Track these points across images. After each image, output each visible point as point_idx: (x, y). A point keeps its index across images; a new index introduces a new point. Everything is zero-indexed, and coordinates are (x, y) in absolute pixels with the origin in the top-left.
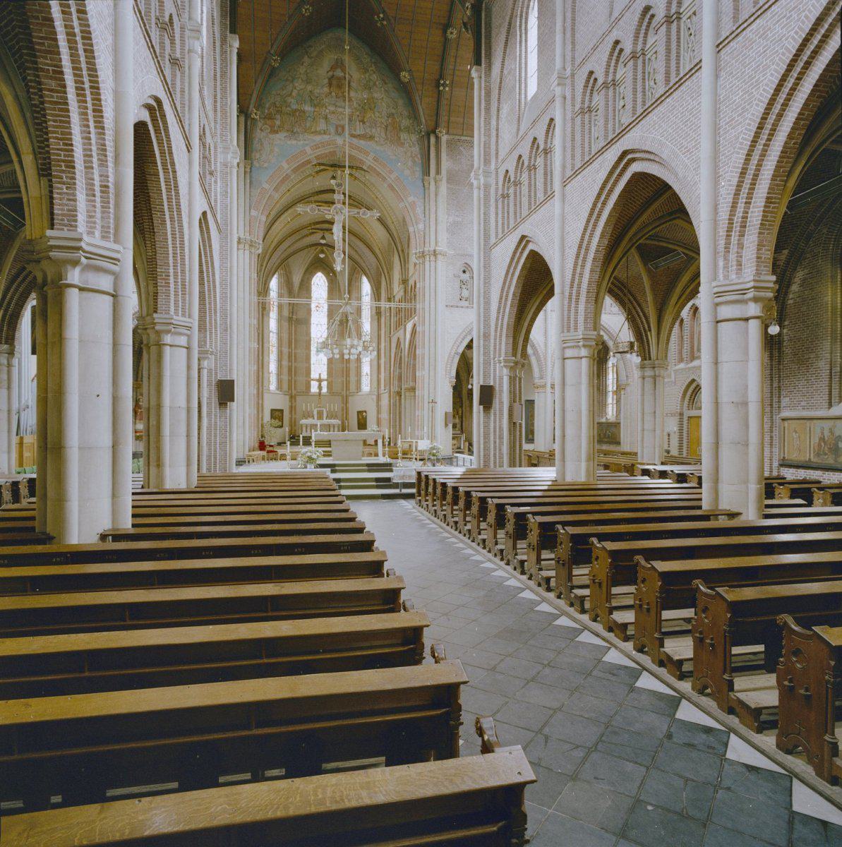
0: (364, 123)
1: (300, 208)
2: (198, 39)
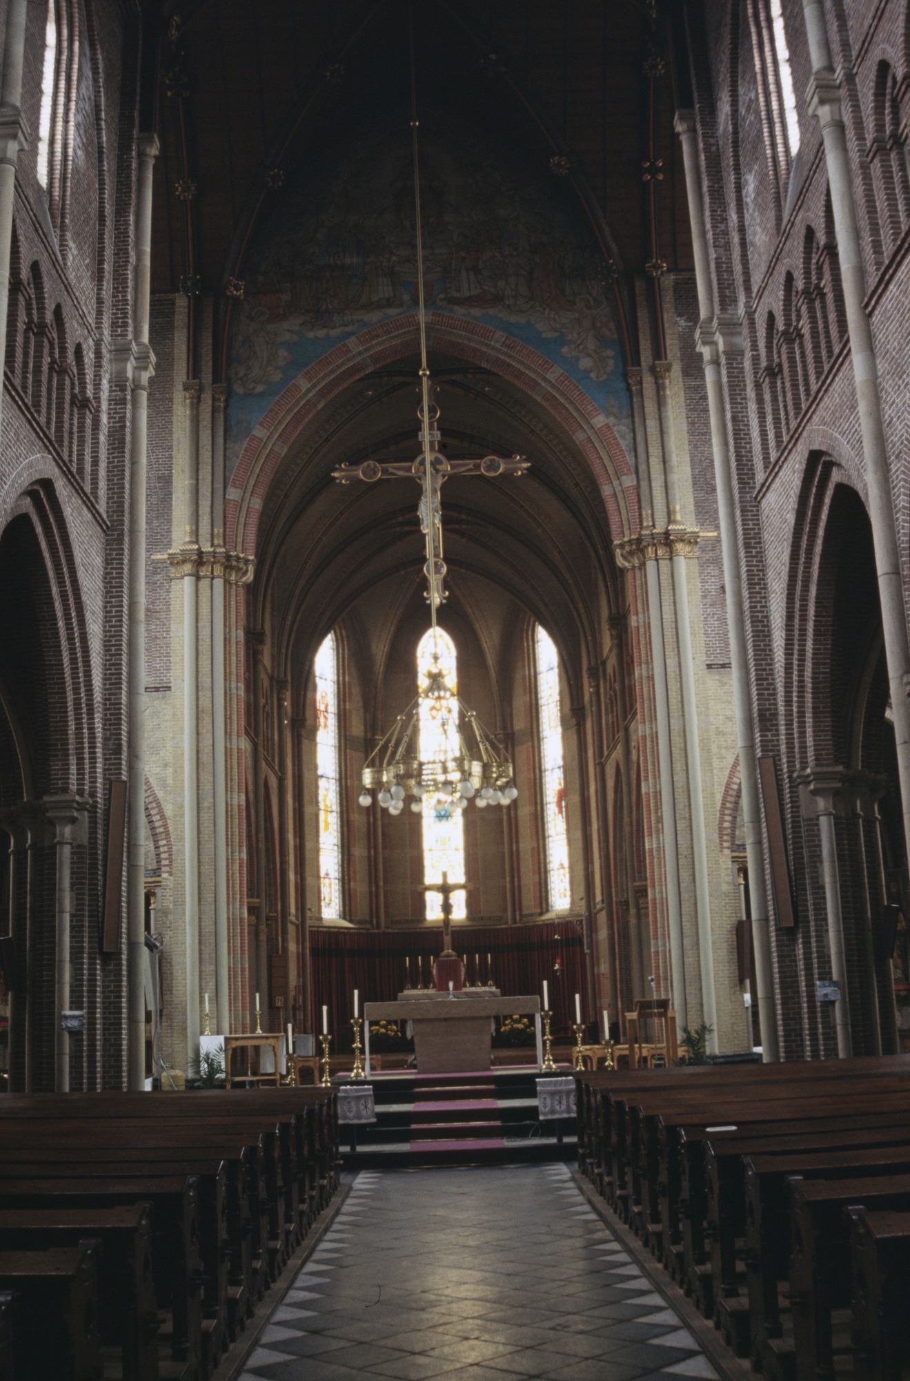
2: (15, 137)
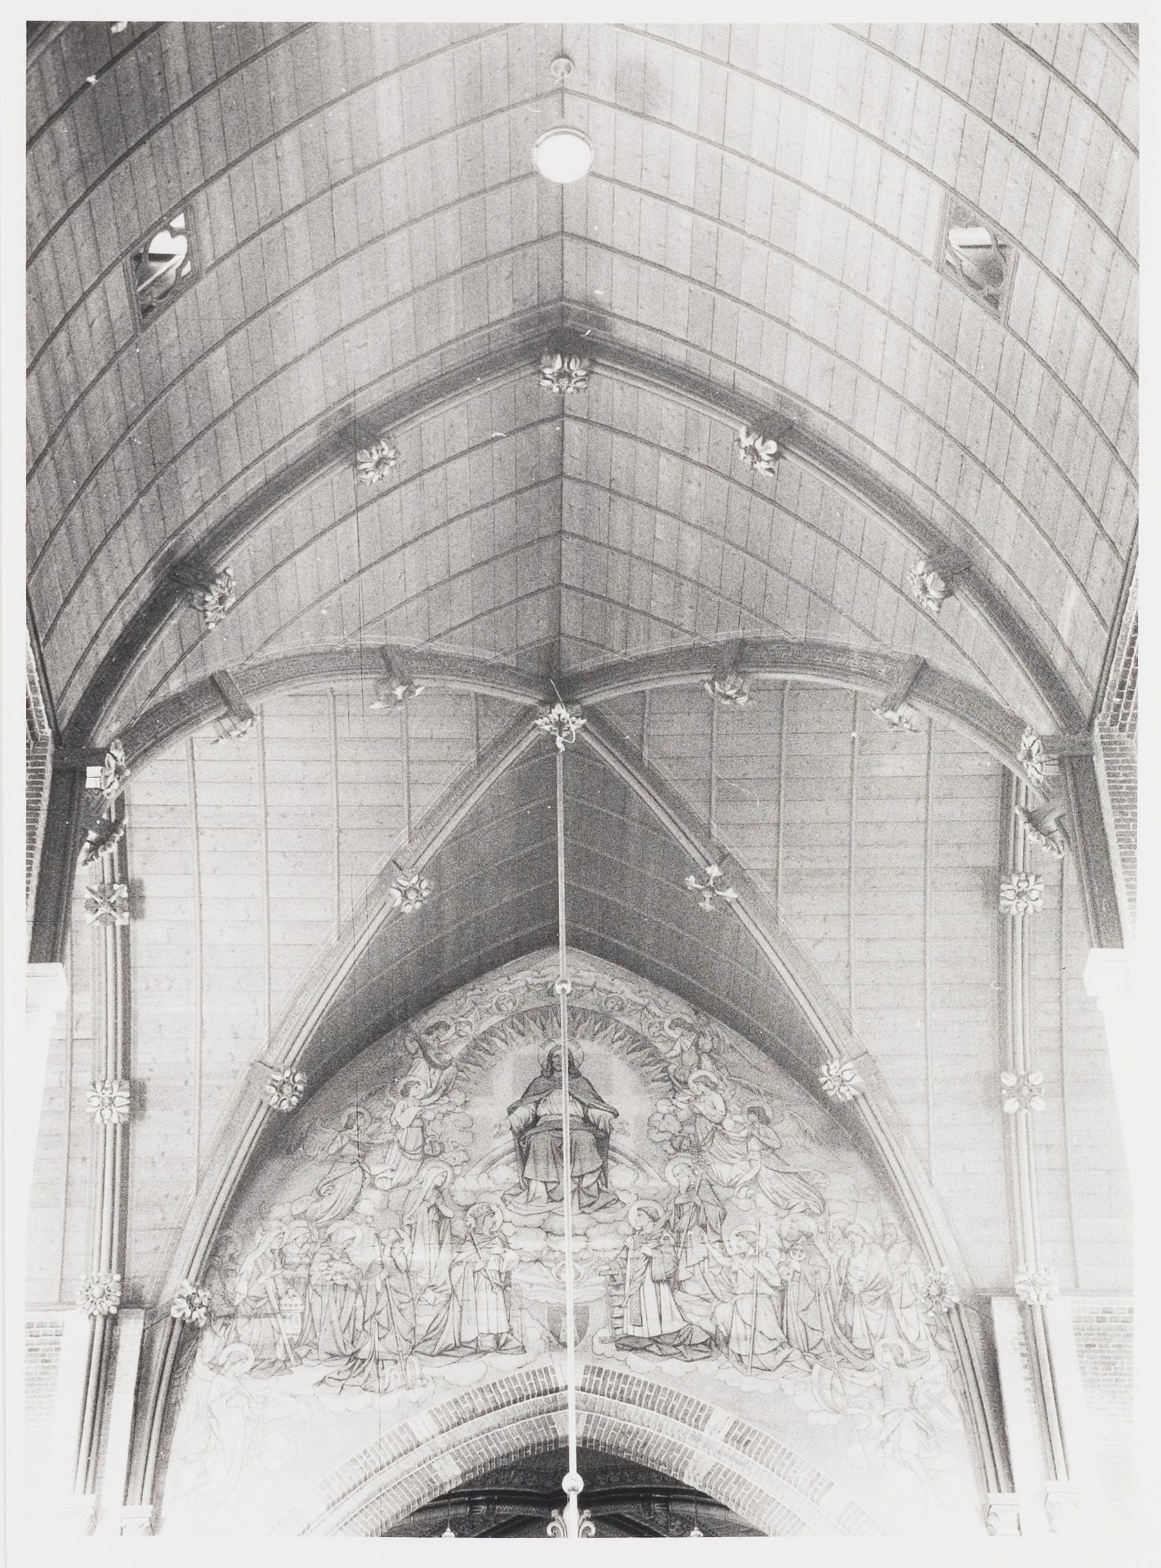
0: (673, 1282)
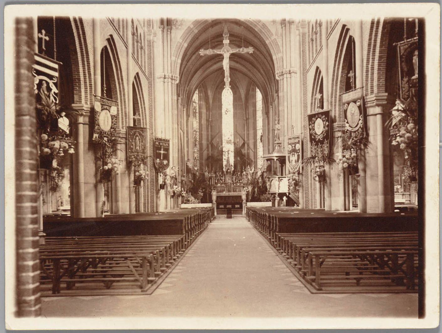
1: (202, 52)
